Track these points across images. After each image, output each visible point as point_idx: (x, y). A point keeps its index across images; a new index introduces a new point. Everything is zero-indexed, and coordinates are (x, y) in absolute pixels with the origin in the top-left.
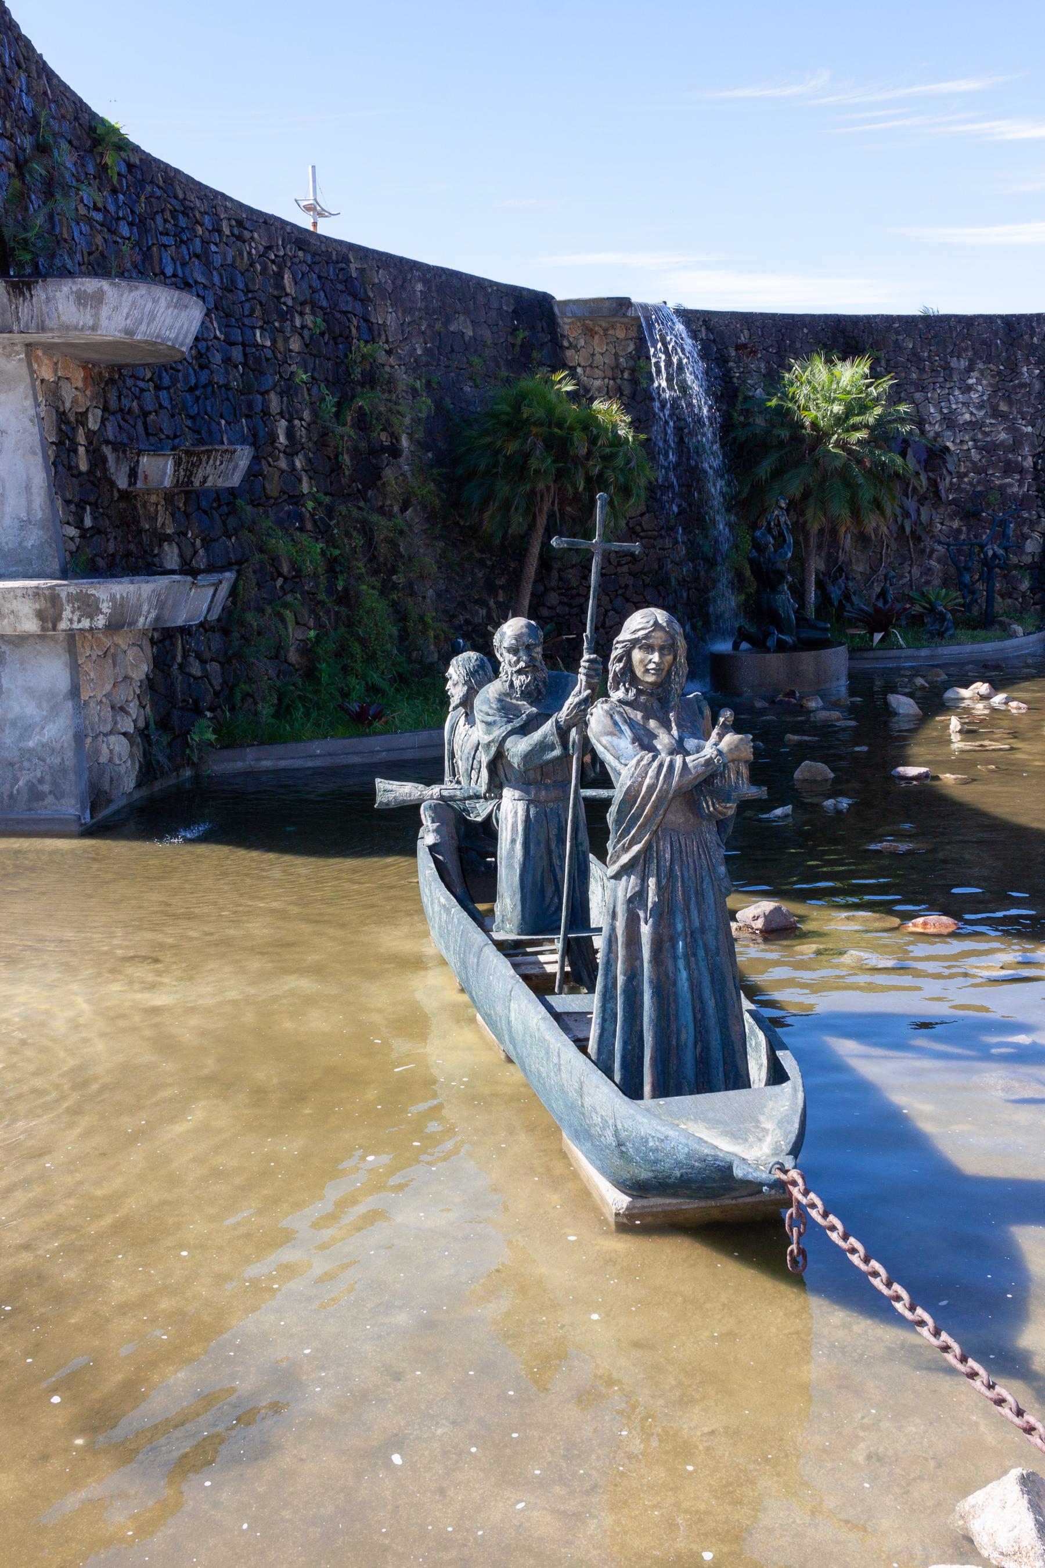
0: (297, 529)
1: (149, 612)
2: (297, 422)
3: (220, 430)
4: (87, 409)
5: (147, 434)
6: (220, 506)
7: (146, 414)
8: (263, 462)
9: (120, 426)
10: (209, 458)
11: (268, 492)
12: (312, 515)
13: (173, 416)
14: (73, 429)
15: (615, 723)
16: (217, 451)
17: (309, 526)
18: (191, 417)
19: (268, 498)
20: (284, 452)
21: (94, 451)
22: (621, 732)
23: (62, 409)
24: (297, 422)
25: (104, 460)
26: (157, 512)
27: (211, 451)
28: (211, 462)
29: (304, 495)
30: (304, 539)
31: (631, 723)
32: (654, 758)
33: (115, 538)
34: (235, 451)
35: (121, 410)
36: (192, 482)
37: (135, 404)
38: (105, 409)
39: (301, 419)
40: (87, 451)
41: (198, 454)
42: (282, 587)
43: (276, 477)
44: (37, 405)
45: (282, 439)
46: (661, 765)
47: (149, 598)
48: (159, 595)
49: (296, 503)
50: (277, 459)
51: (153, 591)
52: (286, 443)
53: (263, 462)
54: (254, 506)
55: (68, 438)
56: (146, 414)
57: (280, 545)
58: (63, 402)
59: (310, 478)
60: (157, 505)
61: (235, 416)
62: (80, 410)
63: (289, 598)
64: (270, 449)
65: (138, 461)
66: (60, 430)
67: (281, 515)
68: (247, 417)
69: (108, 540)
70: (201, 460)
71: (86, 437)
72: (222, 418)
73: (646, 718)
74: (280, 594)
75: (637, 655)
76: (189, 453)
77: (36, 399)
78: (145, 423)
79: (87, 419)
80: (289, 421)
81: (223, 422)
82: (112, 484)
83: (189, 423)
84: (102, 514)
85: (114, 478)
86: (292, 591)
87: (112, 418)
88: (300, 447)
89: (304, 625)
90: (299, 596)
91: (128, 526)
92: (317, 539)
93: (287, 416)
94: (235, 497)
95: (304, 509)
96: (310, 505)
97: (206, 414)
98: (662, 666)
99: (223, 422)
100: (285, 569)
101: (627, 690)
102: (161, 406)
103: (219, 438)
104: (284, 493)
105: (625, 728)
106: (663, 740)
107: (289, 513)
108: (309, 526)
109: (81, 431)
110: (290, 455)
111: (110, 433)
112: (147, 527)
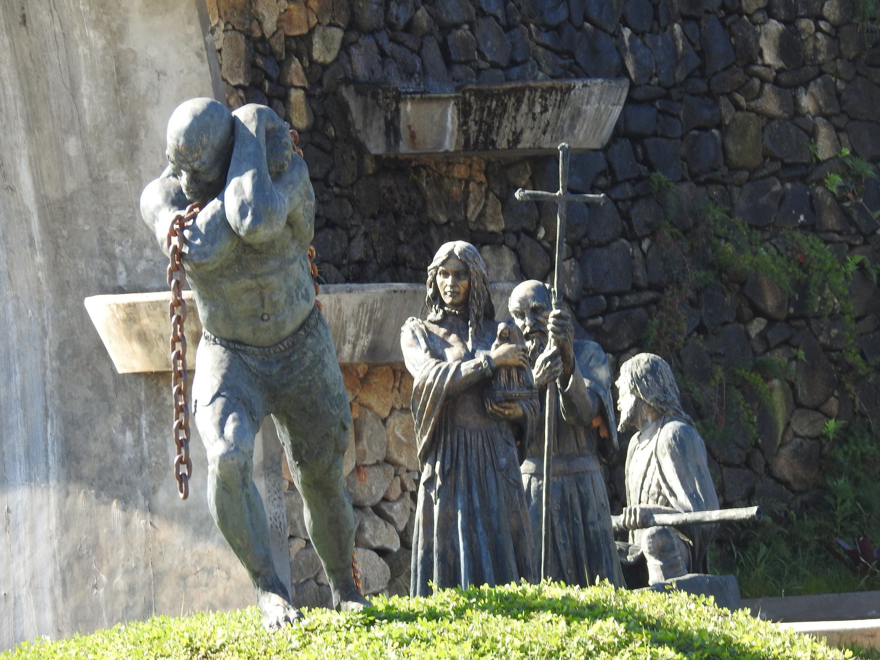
0: (802, 227)
1: (357, 337)
2: (806, 24)
3: (620, 49)
4: (311, 31)
5: (449, 62)
6: (615, 183)
7: (446, 28)
8: (724, 101)
9: (383, 53)
10: (519, 101)
11: (733, 157)
12: (839, 200)
13: (508, 28)
14: (280, 64)
15: (415, 337)
16: (533, 89)
17: (831, 221)
18: (549, 28)
19: (733, 169)
20: (776, 82)
21: (325, 95)
22: (418, 343)
23: (257, 34)
24: (806, 24)
25: (344, 109)
26: (466, 193)
27: (522, 90)
28: (524, 108)
29: (819, 162)
30: (813, 247)
31: (429, 337)
32: (437, 363)
33: (366, 235)
34: (569, 89)
35: (390, 26)
36: (493, 143)
37: (422, 14)
38: (352, 26)
39: (818, 17)
40: (309, 96)
41: (498, 96)
42: (762, 335)
43: (753, 131)
44: (207, 29)
45: (769, 57)
46: (440, 369)
47: (356, 316)
48: (372, 312)
49: (803, 179)
50: (760, 94)
51: (361, 305)
52: (780, 64)
53: (724, 101)
54: (698, 184)
55: (268, 77)
56: (446, 28)
57: (762, 260)
58: (260, 24)
59: (838, 130)
60: (467, 183)
61: (656, 18)
62: (296, 32)
63: (778, 357)
64: (740, 77)
65: (397, 110)
66: (253, 65)
67: (764, 200)
68: (685, 19)
69: (350, 240)
70: (504, 107)
71: (307, 75)
72: (626, 25)
73: (448, 334)
74: (759, 348)
75: (440, 279)
76: (478, 93)
77: (204, 20)
78: (444, 48)
79: (310, 46)
80: (790, 22)
81: (627, 32)
82: (361, 149)
83: (546, 38)
84: (336, 196)
85: (362, 137)
86: (787, 343)
87: (367, 42)
88: (812, 71)
89: (816, 409)
90: (801, 354)
91: (397, 215)
92: (852, 247)
93: (782, 13)
94: (652, 168)
95: (819, 190)
96: (835, 181)
97: (587, 19)
98: (457, 289)
99: (627, 32)
100: (770, 302)
101: (437, 312)
102: (481, 13)
103: (616, 60)
104: (774, 159)
105: (422, 341)
106: (453, 352)
107: (782, 199)
108: (831, 221)
109: (296, 65)
110: (788, 83)
111: (360, 65)
112: (443, 219)
